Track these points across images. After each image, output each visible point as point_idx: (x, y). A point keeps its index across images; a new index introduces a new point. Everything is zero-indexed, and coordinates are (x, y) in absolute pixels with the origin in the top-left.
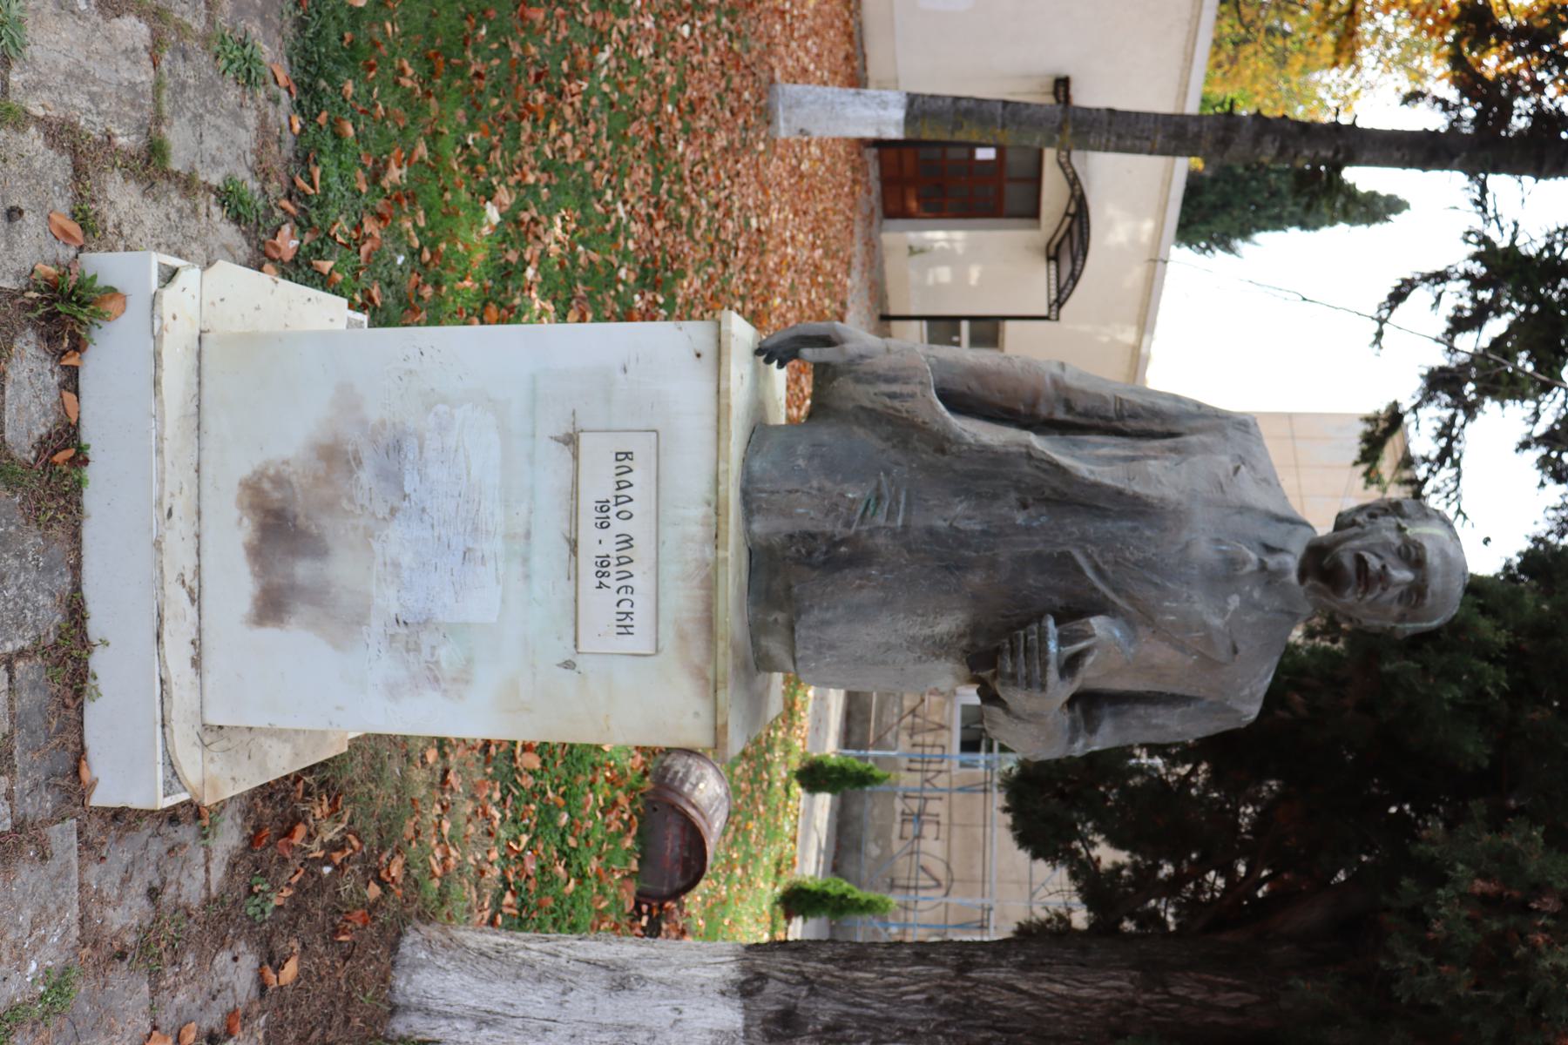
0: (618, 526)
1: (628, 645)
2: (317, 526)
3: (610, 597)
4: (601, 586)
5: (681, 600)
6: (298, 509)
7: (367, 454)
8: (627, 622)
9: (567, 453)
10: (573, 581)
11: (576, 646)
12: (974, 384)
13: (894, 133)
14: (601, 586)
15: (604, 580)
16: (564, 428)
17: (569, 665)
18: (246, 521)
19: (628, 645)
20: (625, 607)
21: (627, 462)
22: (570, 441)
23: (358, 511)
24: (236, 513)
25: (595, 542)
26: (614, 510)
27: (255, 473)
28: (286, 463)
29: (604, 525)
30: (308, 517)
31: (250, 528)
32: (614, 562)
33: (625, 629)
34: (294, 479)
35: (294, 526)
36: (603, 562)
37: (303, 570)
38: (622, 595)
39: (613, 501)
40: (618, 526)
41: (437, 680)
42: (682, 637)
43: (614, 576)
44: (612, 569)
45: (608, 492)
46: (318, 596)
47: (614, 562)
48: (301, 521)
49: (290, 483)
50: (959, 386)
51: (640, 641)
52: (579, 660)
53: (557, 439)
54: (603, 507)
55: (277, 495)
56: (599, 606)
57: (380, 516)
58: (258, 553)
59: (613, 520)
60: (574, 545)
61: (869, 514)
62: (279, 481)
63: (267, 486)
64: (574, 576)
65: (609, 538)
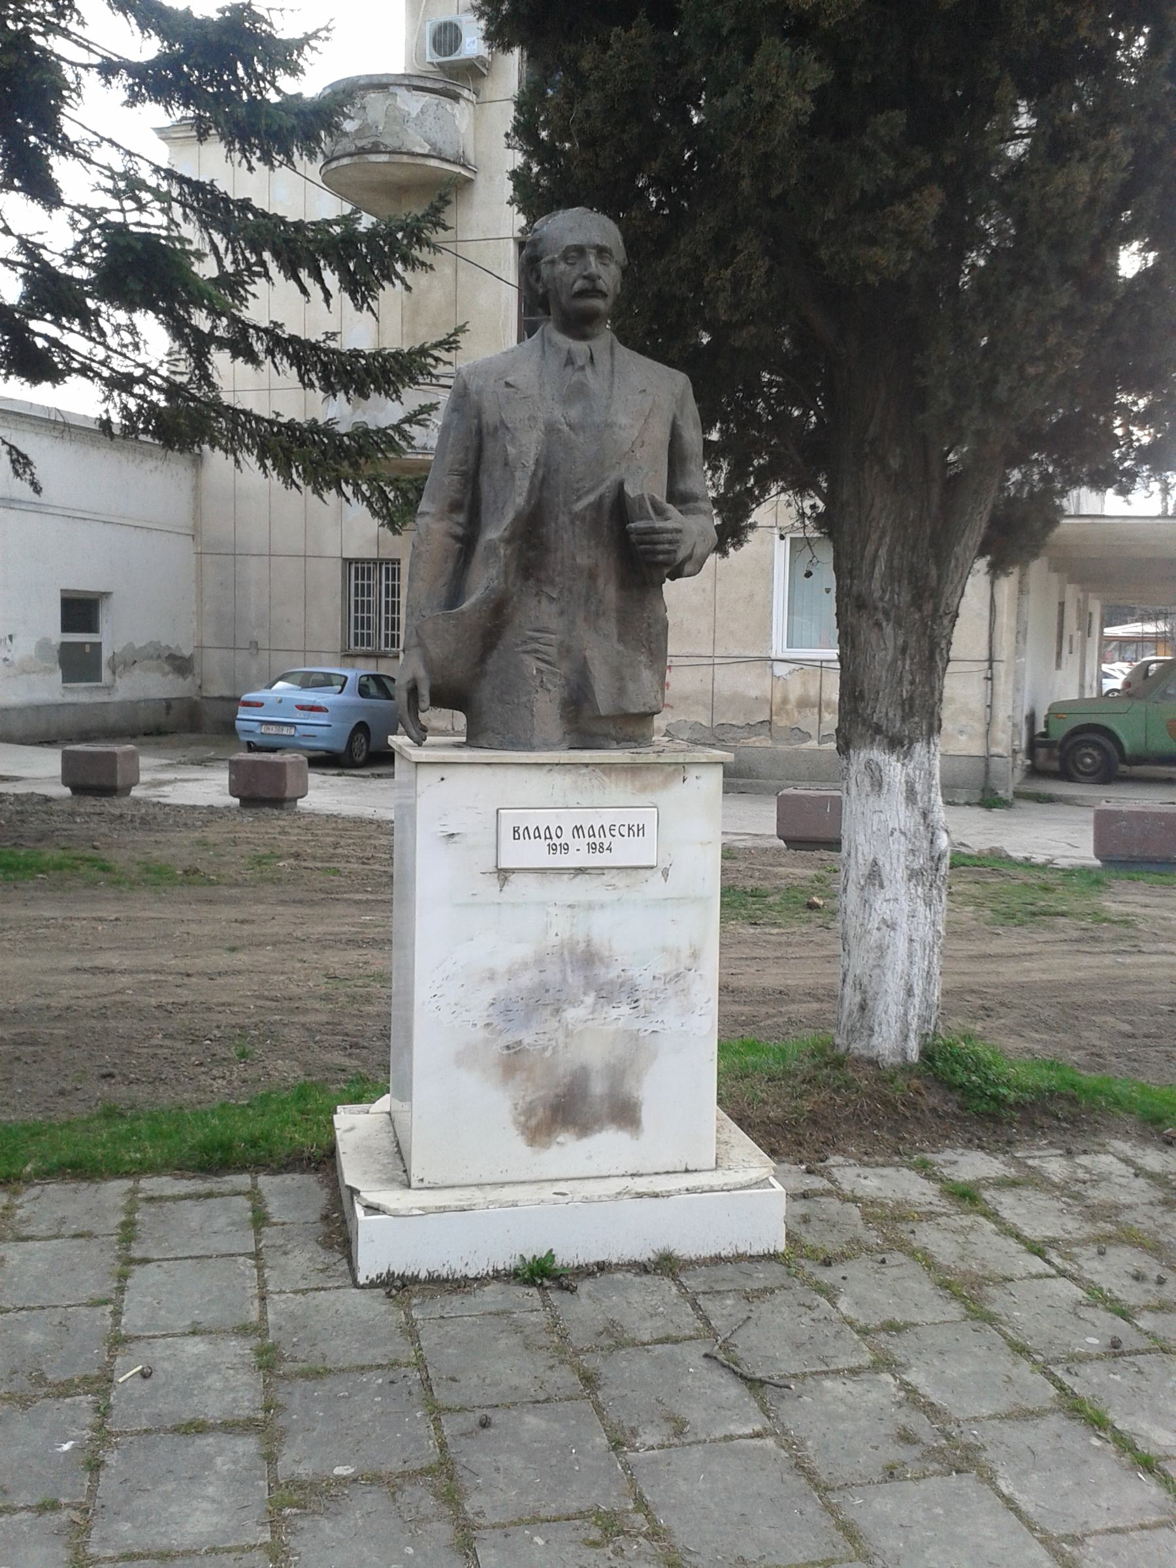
0: (567, 838)
1: (651, 829)
2: (564, 1077)
3: (617, 842)
4: (609, 849)
5: (618, 791)
6: (552, 1094)
7: (509, 1039)
8: (635, 829)
9: (513, 877)
10: (606, 871)
11: (652, 868)
12: (443, 580)
13: (670, 589)
14: (609, 849)
15: (605, 847)
16: (494, 880)
17: (665, 873)
18: (560, 1139)
19: (651, 829)
20: (624, 831)
21: (521, 832)
22: (503, 874)
23: (554, 1043)
24: (554, 1149)
25: (579, 857)
26: (555, 840)
27: (523, 1133)
28: (516, 1105)
29: (566, 848)
30: (557, 1086)
31: (566, 1135)
32: (592, 840)
33: (641, 829)
34: (528, 1099)
35: (564, 1097)
36: (592, 847)
37: (598, 1087)
38: (616, 833)
39: (549, 841)
40: (567, 838)
41: (678, 975)
42: (643, 789)
43: (602, 839)
44: (597, 840)
45: (543, 843)
46: (618, 1073)
47: (592, 840)
48: (559, 1091)
49: (531, 1103)
50: (443, 592)
51: (647, 817)
52: (662, 866)
53: (502, 887)
54: (553, 848)
55: (540, 1113)
56: (625, 852)
57: (557, 1024)
58: (584, 1129)
59: (562, 841)
60: (580, 871)
61: (547, 658)
62: (529, 1111)
63: (533, 1122)
64: (601, 870)
65: (582, 842)
